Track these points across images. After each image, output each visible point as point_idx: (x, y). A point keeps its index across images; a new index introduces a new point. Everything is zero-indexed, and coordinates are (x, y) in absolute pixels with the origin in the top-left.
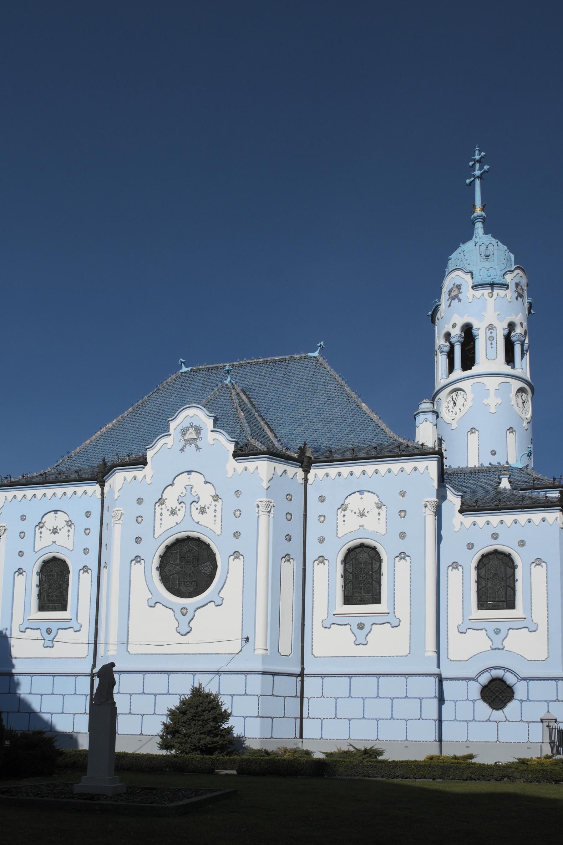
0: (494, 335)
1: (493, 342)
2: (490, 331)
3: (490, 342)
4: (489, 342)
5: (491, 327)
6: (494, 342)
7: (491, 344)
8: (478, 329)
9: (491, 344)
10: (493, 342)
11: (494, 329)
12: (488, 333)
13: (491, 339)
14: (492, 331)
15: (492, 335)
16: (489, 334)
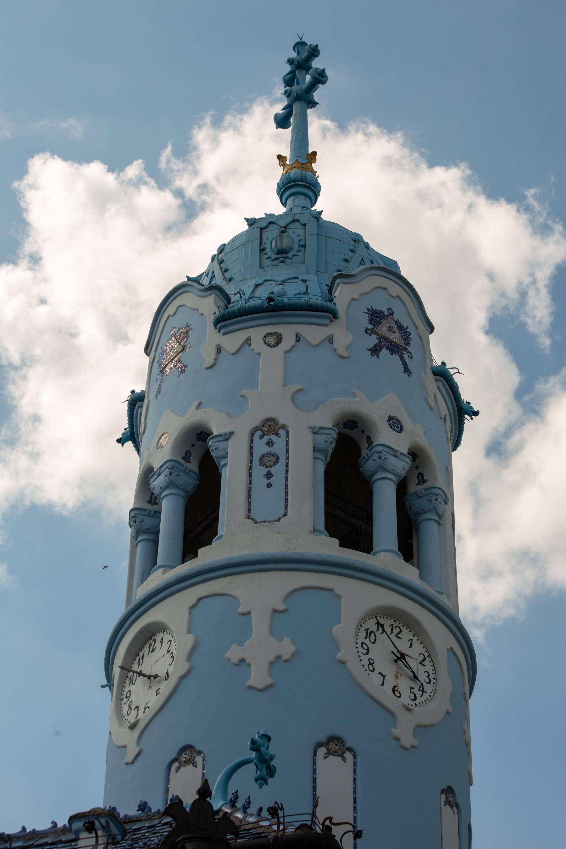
0: (278, 448)
1: (273, 470)
2: (266, 438)
3: (264, 471)
4: (259, 471)
5: (270, 427)
6: (278, 470)
7: (269, 475)
8: (227, 437)
9: (269, 475)
10: (273, 470)
11: (282, 432)
13: (269, 460)
14: (273, 437)
15: (273, 450)
16: (261, 447)
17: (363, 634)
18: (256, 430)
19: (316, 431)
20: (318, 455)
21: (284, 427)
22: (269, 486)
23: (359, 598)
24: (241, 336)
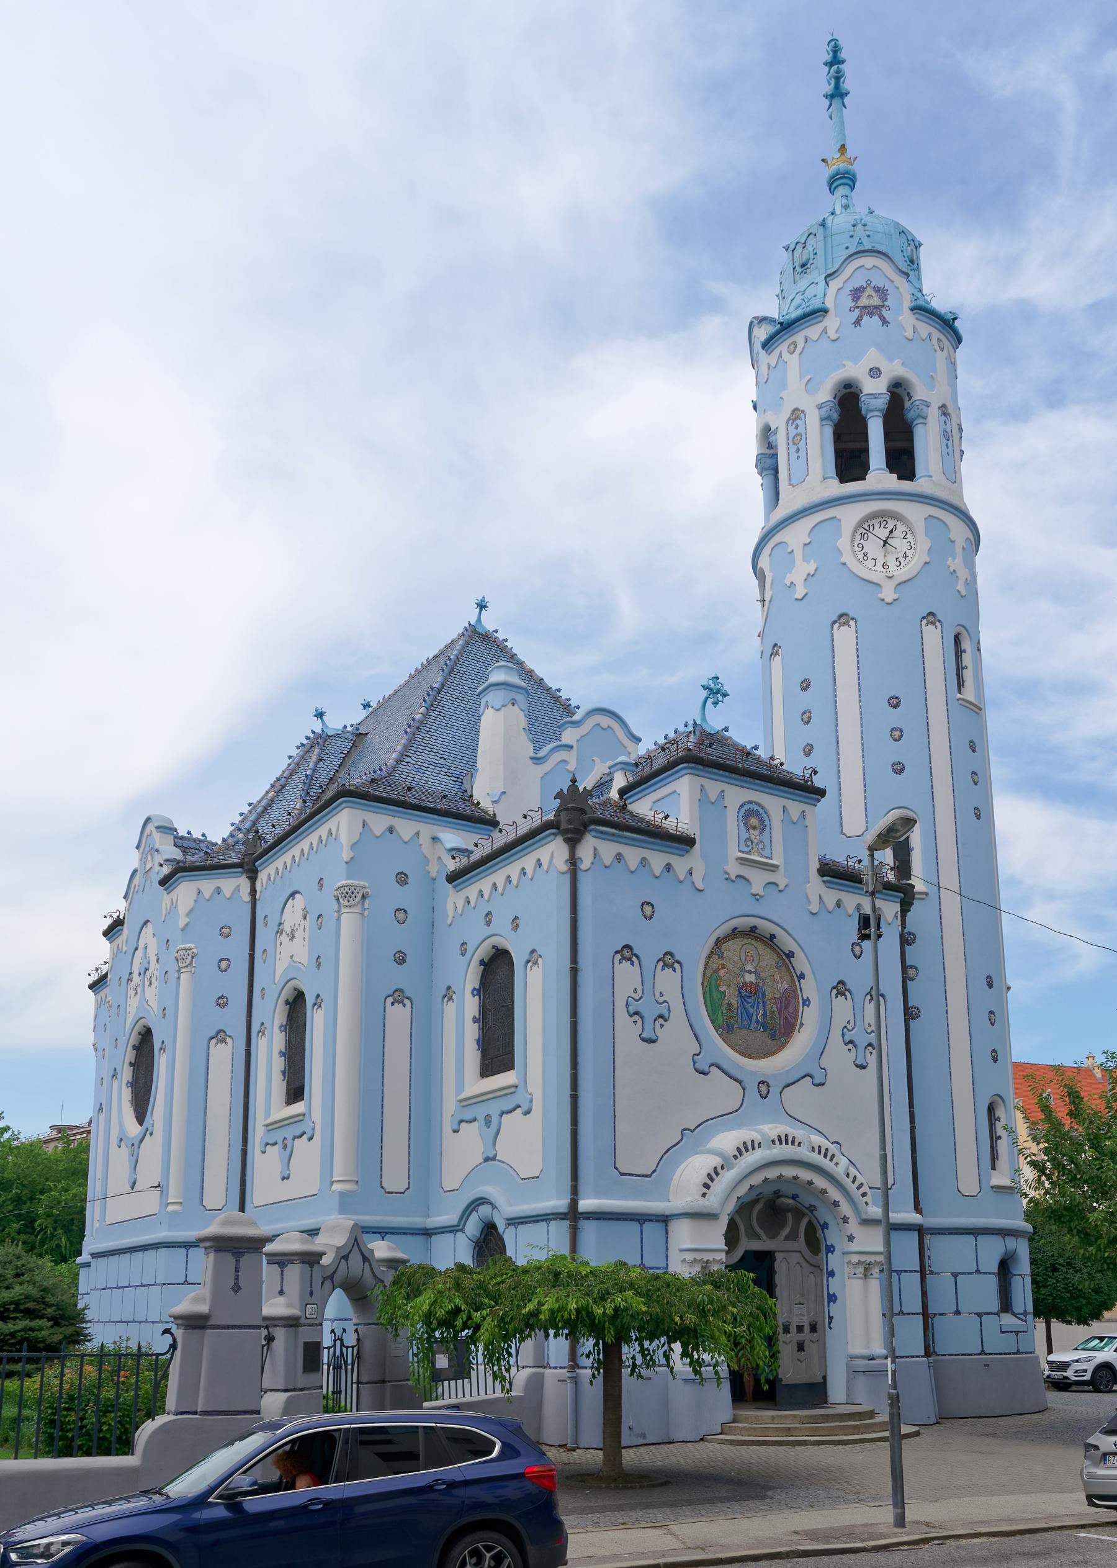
0: (801, 430)
3: (795, 448)
4: (793, 448)
5: (796, 414)
6: (802, 445)
7: (798, 450)
9: (798, 450)
11: (802, 416)
12: (792, 428)
14: (798, 421)
15: (799, 431)
16: (793, 432)
17: (858, 537)
18: (789, 419)
19: (820, 407)
20: (825, 422)
21: (803, 411)
22: (798, 458)
23: (851, 515)
24: (776, 353)
